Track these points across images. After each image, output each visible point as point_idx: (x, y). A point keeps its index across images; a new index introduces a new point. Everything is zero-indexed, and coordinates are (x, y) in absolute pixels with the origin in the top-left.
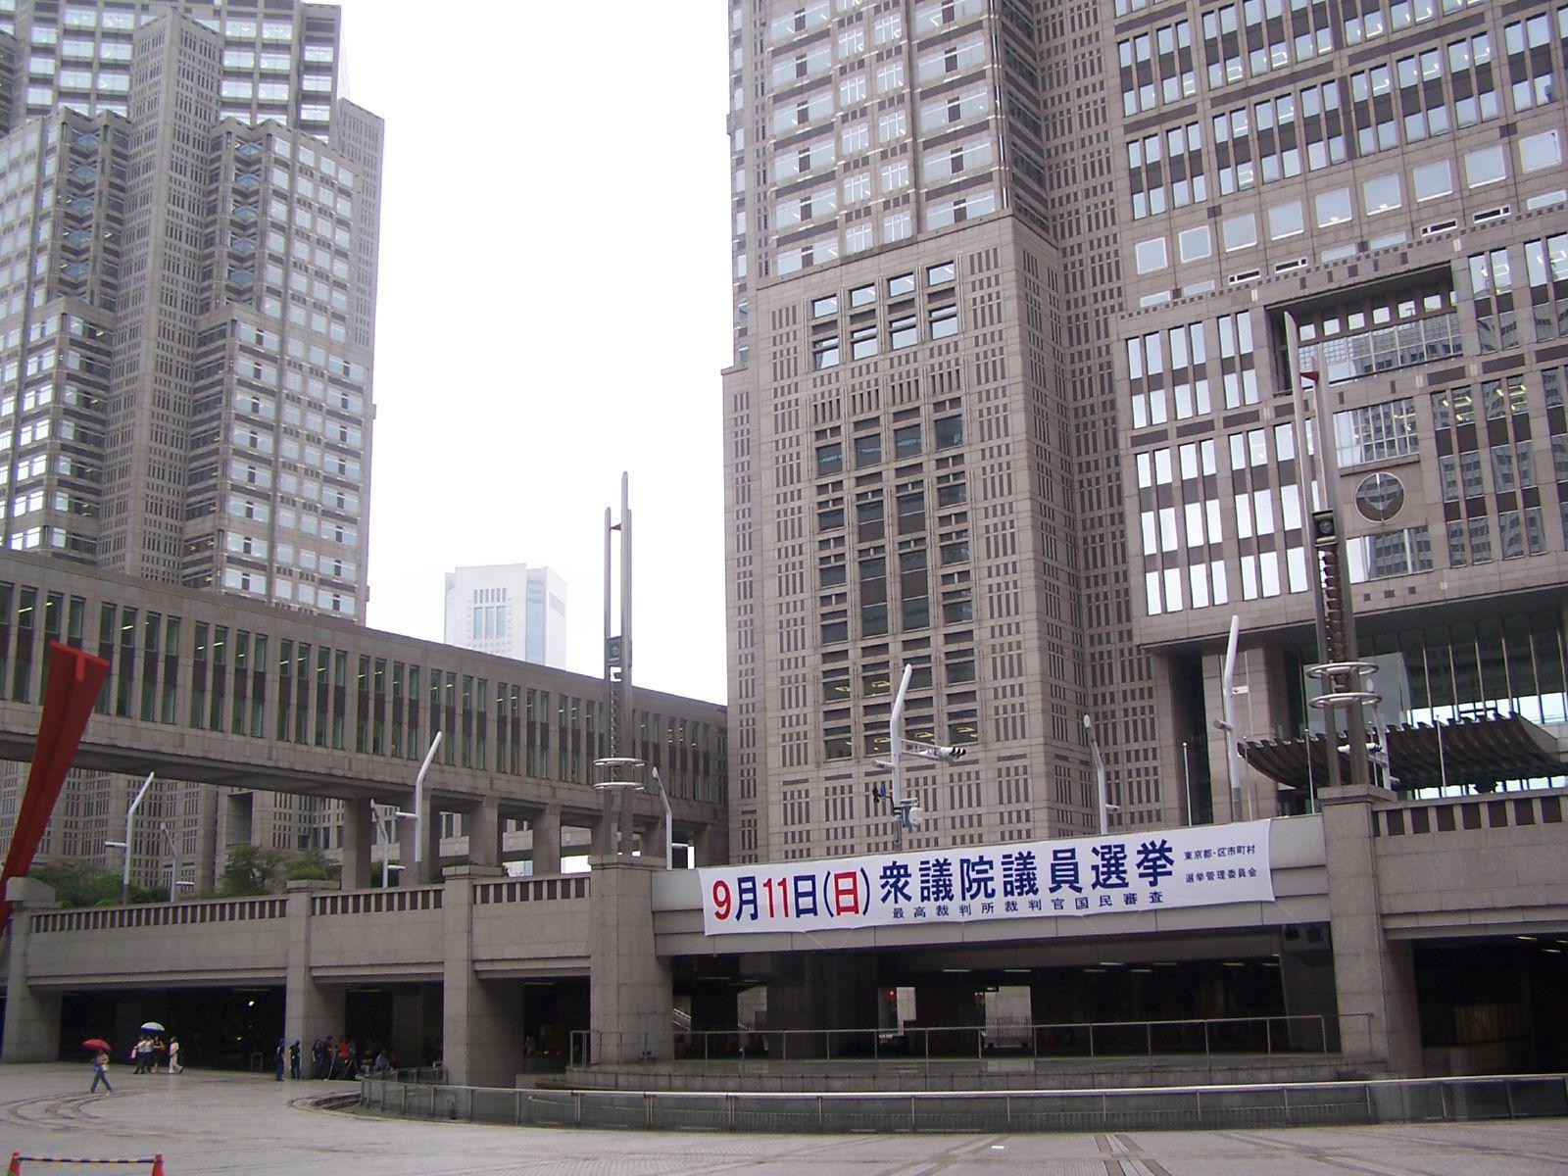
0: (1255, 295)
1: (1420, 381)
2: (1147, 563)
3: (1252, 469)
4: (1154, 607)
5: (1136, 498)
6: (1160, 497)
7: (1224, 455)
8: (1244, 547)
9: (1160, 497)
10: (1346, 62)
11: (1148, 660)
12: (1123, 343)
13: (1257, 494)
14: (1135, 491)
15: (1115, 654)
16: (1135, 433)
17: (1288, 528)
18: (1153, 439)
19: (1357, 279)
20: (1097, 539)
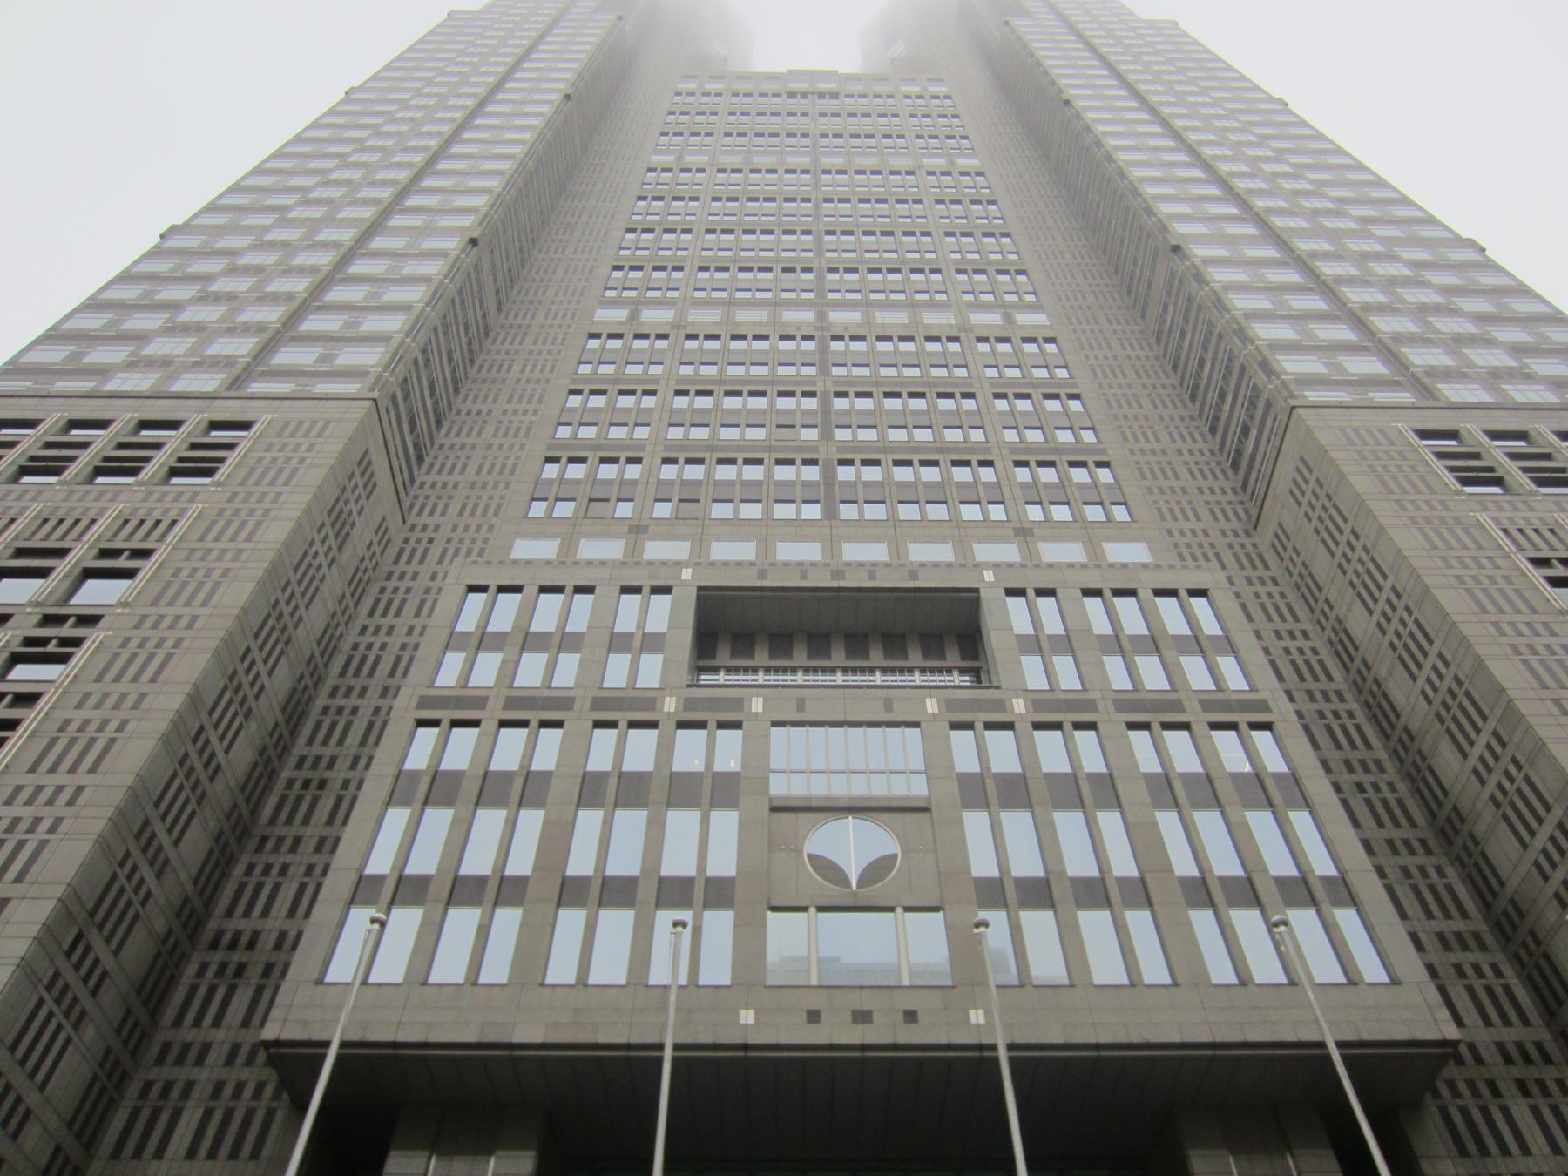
0: (687, 574)
1: (932, 706)
2: (364, 889)
3: (621, 775)
4: (342, 969)
5: (390, 781)
6: (439, 787)
7: (576, 751)
8: (571, 892)
9: (439, 787)
10: (834, 449)
11: (270, 1114)
12: (463, 588)
13: (620, 814)
14: (393, 770)
15: (200, 1093)
16: (432, 692)
17: (666, 871)
18: (459, 712)
19: (843, 584)
20: (275, 871)
